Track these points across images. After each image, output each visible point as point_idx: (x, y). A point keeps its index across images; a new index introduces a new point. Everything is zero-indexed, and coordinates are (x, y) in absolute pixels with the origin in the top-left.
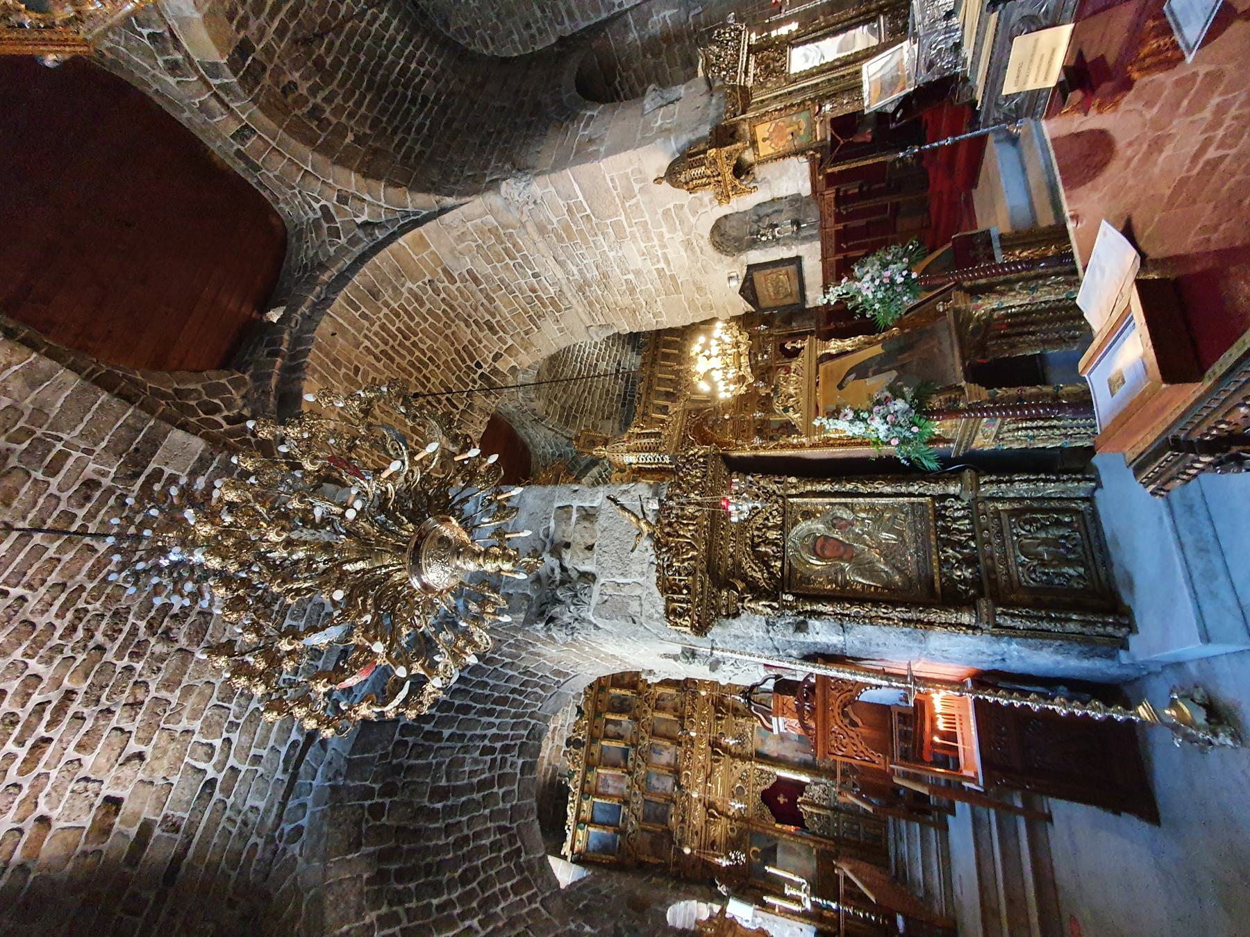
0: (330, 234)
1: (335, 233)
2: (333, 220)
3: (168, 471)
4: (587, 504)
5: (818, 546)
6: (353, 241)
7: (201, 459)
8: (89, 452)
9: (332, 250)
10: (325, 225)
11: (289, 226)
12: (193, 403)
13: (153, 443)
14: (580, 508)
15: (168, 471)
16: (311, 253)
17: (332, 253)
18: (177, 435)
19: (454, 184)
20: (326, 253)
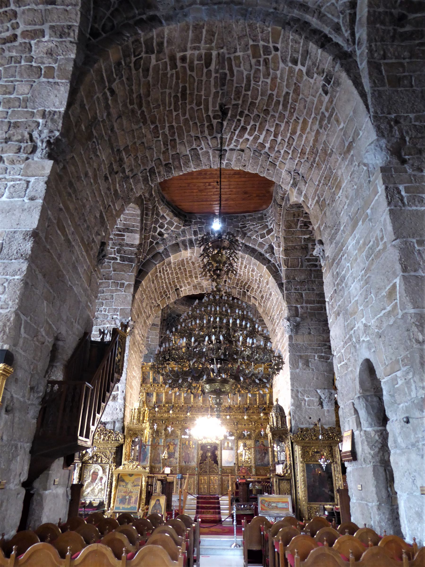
0: (261, 234)
1: (263, 236)
2: (268, 235)
3: (125, 237)
4: (119, 397)
5: (95, 474)
6: (261, 245)
7: (132, 245)
8: (121, 221)
9: (254, 237)
10: (265, 232)
11: (264, 212)
12: (161, 221)
13: (132, 231)
14: (117, 394)
15: (125, 237)
16: (252, 227)
17: (252, 238)
18: (137, 236)
19: (295, 289)
20: (252, 235)
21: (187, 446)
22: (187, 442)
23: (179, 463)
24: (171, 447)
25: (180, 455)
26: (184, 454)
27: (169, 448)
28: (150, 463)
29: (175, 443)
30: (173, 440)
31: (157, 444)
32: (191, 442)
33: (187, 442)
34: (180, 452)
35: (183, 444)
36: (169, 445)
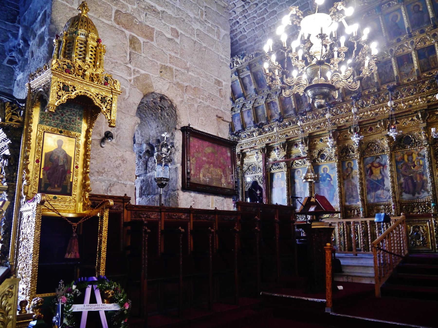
21: (406, 164)
22: (406, 157)
23: (394, 197)
24: (376, 172)
25: (393, 182)
26: (402, 180)
27: (372, 173)
28: (341, 202)
29: (383, 163)
30: (377, 157)
31: (349, 169)
32: (415, 156)
33: (406, 157)
34: (392, 177)
35: (397, 162)
36: (370, 168)
